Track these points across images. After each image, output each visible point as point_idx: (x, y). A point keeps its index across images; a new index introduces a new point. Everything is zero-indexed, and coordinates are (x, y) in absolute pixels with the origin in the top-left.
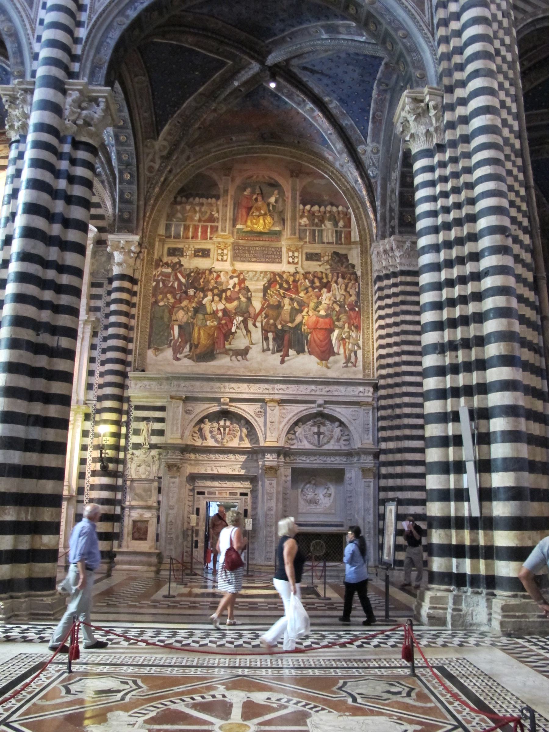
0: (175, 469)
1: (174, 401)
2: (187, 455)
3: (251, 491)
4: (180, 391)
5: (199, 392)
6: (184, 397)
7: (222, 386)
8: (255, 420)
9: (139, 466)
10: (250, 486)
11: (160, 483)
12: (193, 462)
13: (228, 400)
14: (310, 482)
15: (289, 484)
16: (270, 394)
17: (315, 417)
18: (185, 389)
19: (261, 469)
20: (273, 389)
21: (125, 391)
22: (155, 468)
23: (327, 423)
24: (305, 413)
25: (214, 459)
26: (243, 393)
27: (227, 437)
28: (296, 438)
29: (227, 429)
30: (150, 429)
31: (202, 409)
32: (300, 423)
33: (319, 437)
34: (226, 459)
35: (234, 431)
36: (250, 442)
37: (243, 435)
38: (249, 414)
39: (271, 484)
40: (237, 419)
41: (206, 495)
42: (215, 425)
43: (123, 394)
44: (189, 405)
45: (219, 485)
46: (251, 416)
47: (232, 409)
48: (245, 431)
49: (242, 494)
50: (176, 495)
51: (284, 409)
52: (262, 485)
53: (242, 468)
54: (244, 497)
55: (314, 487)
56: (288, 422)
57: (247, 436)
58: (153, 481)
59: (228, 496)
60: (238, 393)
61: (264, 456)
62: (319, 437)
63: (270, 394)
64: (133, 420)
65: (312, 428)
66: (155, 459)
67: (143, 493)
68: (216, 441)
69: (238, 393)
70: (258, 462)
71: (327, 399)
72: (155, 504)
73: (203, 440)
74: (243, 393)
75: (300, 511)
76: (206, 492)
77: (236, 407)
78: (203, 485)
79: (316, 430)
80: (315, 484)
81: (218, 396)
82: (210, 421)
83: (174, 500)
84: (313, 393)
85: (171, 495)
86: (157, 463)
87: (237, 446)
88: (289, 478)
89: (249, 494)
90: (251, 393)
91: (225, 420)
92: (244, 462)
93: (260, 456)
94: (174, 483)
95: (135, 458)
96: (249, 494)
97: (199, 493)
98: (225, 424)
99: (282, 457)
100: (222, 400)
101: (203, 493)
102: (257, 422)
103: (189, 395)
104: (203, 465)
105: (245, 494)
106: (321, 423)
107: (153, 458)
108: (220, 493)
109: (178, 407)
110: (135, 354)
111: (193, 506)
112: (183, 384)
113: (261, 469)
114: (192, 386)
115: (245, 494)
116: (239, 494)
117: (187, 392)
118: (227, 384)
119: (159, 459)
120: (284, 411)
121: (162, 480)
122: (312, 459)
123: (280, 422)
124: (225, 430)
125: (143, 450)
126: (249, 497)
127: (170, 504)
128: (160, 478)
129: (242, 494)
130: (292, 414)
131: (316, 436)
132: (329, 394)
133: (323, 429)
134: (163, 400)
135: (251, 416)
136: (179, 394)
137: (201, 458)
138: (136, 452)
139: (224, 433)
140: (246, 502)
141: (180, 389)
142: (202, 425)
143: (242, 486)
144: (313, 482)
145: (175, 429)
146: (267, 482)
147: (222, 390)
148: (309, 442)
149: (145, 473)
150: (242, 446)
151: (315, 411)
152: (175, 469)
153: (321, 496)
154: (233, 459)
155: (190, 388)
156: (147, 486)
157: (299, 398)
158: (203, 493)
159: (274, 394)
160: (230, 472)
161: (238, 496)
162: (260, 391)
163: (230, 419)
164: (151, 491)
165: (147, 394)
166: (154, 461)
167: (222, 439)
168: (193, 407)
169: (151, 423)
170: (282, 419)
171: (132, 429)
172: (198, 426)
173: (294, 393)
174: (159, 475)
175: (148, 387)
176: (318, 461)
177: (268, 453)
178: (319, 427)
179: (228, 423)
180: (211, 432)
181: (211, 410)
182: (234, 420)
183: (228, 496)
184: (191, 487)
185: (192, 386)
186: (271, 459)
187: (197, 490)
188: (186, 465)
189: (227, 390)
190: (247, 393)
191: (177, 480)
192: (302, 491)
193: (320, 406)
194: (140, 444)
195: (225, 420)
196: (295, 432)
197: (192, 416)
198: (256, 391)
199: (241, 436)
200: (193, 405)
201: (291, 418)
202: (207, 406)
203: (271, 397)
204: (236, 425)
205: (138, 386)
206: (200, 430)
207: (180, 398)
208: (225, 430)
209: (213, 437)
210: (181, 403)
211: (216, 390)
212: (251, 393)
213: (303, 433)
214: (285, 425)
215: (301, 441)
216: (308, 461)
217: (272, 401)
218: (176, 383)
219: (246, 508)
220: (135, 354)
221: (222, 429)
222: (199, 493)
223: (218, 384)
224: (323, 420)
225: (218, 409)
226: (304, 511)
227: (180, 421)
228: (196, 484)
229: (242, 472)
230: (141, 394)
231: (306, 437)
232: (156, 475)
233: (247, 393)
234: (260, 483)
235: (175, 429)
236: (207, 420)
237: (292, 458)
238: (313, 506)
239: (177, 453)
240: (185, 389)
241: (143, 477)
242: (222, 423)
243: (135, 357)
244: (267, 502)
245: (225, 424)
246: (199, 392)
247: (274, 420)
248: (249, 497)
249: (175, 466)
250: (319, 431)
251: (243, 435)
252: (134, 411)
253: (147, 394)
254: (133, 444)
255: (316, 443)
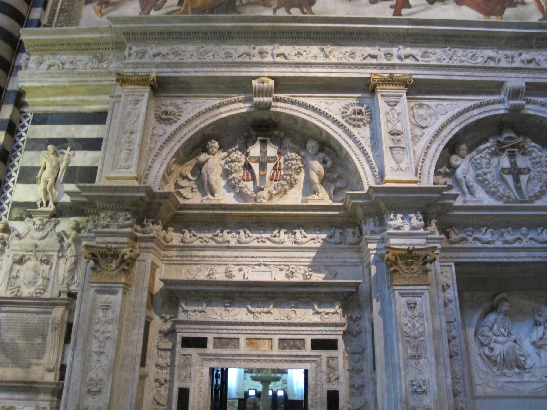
0: (114, 265)
1: (129, 88)
2: (156, 230)
3: (345, 334)
4: (143, 65)
5: (194, 65)
6: (153, 75)
7: (256, 52)
8: (347, 132)
9: (21, 261)
10: (344, 320)
11: (70, 310)
12: (173, 253)
13: (272, 83)
14: (493, 309)
15: (455, 306)
16: (381, 66)
17: (500, 133)
18: (158, 60)
19: (376, 262)
20: (388, 55)
21: (12, 78)
22: (64, 267)
23: (531, 145)
24: (477, 115)
25: (233, 243)
26: (310, 65)
27: (270, 186)
28: (458, 182)
29: (270, 166)
30: (63, 166)
31: (203, 108)
32: (464, 147)
33: (517, 181)
34: (268, 244)
35: (287, 168)
36: (334, 195)
37: (315, 178)
38: (327, 116)
39: (412, 306)
40: (294, 142)
41: (210, 348)
42: (237, 155)
43: (7, 83)
44: (168, 101)
45: (250, 318)
46: (335, 121)
47: (280, 108)
48: (317, 166)
49: (318, 344)
50: (110, 348)
51: (421, 106)
52: (382, 313)
53: (314, 267)
54: (324, 354)
55: (507, 320)
56: (436, 135)
57: (324, 181)
58: (52, 303)
59: (276, 351)
60: (298, 65)
61: (382, 223)
62: (517, 181)
63: (381, 66)
64: (23, 146)
65: (495, 160)
66: (67, 241)
67: (21, 343)
68: (240, 194)
69: (298, 65)
70: (359, 250)
71: (531, 78)
72: (50, 377)
73: (204, 194)
74: (310, 65)
75: (479, 390)
76: (210, 338)
77: (293, 103)
78: (199, 317)
79: (505, 162)
80: (506, 314)
81: (245, 72)
82: (222, 148)
83: (105, 361)
84: (492, 64)
85: (95, 346)
86: (70, 253)
87: (299, 203)
88: (452, 293)
89: (341, 345)
90: (330, 65)
91: (264, 143)
92: (320, 250)
93: (369, 226)
94: (106, 307)
95: (14, 242)
96: (341, 345)
97: (188, 342)
98: (263, 152)
99: (433, 227)
100: (255, 83)
101: (201, 343)
102: (351, 136)
103: (167, 72)
104: (203, 261)
105: (331, 345)
106: (513, 146)
107: (62, 240)
108: (251, 342)
109: (137, 101)
110: (53, 10)
111: (171, 381)
112: (152, 50)
113: (376, 262)
114: (176, 53)
115: (331, 345)
116: (309, 345)
117: (161, 65)
118: (268, 48)
119: (77, 241)
120: (421, 112)
121: (77, 301)
122: (509, 237)
123: (416, 139)
124: (263, 167)
125: (37, 220)
126: (340, 353)
127: (92, 375)
128: (72, 296)
129: (318, 344)
130: (442, 119)
131: (509, 178)
132: (532, 66)
133: (522, 162)
134: (103, 97)
135: (335, 121)
136: (142, 71)
137: (197, 243)
138: (19, 226)
139: (263, 176)
140: (332, 369)
141: (146, 59)
142: (203, 157)
143: (317, 319)
144: (505, 307)
145: (123, 156)
146: (401, 301)
147: (257, 59)
148: (492, 194)
149: (33, 283)
150: (310, 203)
151: (501, 109)
152: (114, 265)
153: (527, 347)
154: (288, 244)
155: (172, 58)
156: (34, 319)
157: (458, 76)
158: (201, 343)
159: (393, 66)
160: (280, 277)
161: (308, 350)
162: (358, 60)
163: (278, 142)
164: (44, 337)
165: (64, 81)
166: (61, 249)
167: (258, 190)
168: (177, 107)
169: (67, 152)
170: (418, 131)
171: (18, 166)
172: (193, 162)
173: (444, 63)
174: (73, 288)
175: (67, 66)
176: (525, 243)
177: (396, 211)
178: (512, 155)
179: (272, 151)
180: (226, 173)
181: (225, 112)
182: (288, 143)
183: (276, 351)
184: (167, 326)
185: (176, 53)
186: (407, 229)
187: (184, 332)
188: (149, 257)
189: (269, 59)
190: (322, 65)
191: (116, 299)
192: (476, 335)
193: (515, 94)
194: (33, 205)
195: (264, 143)
196: (453, 169)
197: (175, 126)
198: (344, 61)
199: (308, 182)
200: (180, 102)
201: (443, 126)
202: (217, 101)
203: (386, 73)
204: (294, 155)
205: (44, 66)
206: (199, 167)
207: (143, 81)
208: (263, 167)
209: (231, 187)
210: (146, 91)
211: (240, 60)
212: (330, 65)
213: (472, 172)
214: (431, 142)
215: (472, 193)
216: (499, 244)
217: (391, 81)
218: (134, 49)
219: (333, 387)
220: (53, 10)
221: (256, 167)
222: (188, 342)
223: (243, 49)
224: (521, 139)
225: (242, 108)
226: (489, 391)
227: (137, 137)
228: (182, 316)
229: (318, 277)
230: (49, 82)
231: (482, 183)
232: (64, 288)
233: (322, 65)
234: (376, 305)
235: (123, 156)
236: (216, 144)
237: (453, 237)
238: (512, 375)
239: (122, 218)
240: (158, 60)
241: (26, 292)
242: (255, 150)
243: (52, 15)
244: (406, 366)
245: (263, 152)
246: (194, 65)
247: (399, 127)
248: (340, 353)
249: (115, 256)
250: (514, 164)
251: (315, 178)
252: (29, 127)
253: (64, 81)
254: (15, 205)
255: (514, 194)
